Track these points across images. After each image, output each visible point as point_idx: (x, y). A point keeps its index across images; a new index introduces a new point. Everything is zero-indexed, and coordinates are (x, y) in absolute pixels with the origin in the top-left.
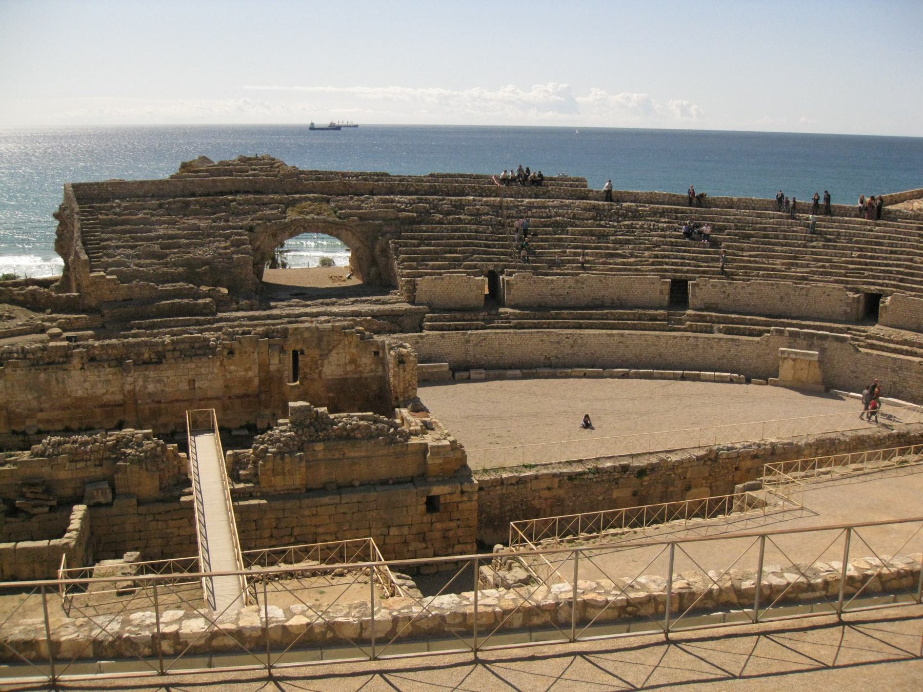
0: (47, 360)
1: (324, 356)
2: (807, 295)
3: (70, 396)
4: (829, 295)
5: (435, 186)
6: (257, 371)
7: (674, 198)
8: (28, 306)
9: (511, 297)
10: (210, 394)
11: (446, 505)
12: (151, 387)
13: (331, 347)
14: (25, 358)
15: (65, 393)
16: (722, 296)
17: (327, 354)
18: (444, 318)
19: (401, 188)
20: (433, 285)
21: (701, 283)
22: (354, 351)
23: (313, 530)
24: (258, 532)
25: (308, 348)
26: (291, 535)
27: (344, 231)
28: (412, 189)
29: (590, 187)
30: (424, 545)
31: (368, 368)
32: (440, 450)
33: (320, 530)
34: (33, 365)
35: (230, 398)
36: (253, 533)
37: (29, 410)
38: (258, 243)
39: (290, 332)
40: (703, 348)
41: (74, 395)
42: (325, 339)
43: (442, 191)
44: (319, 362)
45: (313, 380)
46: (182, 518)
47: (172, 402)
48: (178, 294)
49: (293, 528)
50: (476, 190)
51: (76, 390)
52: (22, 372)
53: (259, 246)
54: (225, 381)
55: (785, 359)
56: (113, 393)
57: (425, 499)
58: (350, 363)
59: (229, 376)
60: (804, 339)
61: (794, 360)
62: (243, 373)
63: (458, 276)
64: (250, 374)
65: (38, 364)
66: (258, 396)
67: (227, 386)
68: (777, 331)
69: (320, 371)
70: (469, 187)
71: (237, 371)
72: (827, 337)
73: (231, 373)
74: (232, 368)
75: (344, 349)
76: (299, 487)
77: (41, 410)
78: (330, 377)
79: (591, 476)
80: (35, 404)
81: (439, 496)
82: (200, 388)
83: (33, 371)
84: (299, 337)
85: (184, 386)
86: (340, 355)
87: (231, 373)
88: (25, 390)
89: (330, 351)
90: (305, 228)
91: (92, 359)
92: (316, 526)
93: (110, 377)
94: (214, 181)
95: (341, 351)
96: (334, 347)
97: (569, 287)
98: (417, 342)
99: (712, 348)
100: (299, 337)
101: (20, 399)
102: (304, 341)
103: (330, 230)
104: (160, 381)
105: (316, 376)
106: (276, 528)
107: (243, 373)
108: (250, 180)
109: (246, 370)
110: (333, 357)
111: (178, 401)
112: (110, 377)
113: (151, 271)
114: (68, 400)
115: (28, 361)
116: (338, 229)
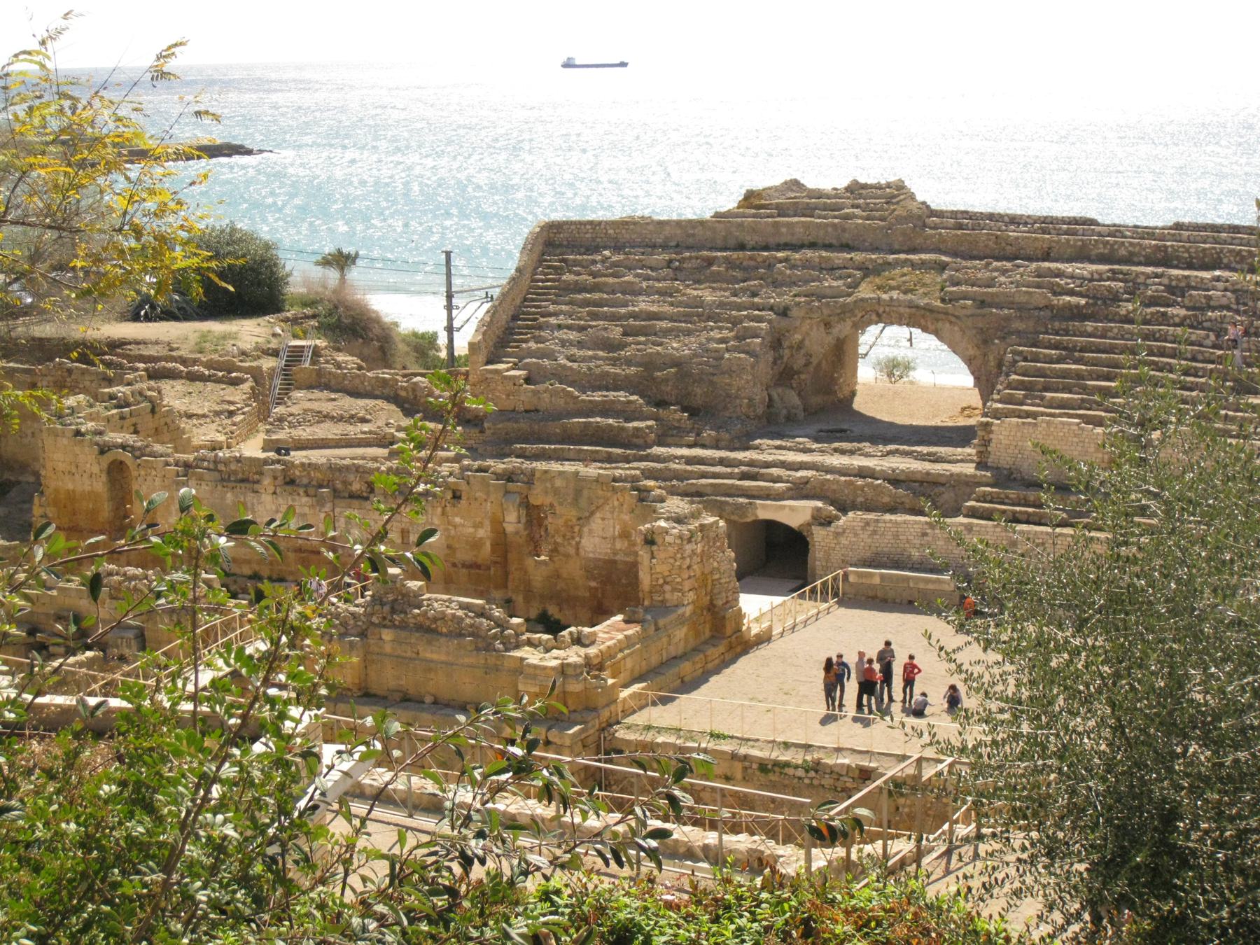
0: (240, 476)
1: (584, 519)
5: (1166, 247)
8: (406, 406)
13: (593, 507)
14: (216, 470)
17: (588, 518)
18: (1007, 497)
19: (1101, 250)
20: (1019, 434)
22: (626, 517)
25: (561, 504)
27: (948, 325)
28: (1123, 252)
32: (538, 672)
34: (223, 480)
38: (798, 337)
39: (537, 475)
42: (585, 493)
43: (1178, 258)
44: (576, 529)
45: (567, 556)
48: (605, 409)
53: (802, 342)
54: (448, 537)
62: (471, 530)
63: (1062, 423)
64: (481, 533)
65: (229, 480)
67: (449, 547)
69: (578, 543)
70: (1231, 251)
71: (463, 526)
73: (455, 527)
74: (458, 520)
75: (612, 513)
78: (591, 555)
79: (800, 773)
83: (219, 487)
89: (592, 513)
90: (878, 315)
91: (291, 482)
94: (776, 225)
95: (609, 515)
98: (924, 534)
100: (548, 485)
102: (556, 492)
103: (923, 323)
105: (572, 551)
107: (471, 530)
108: (834, 225)
110: (597, 523)
112: (306, 510)
113: (585, 369)
115: (216, 474)
116: (937, 320)
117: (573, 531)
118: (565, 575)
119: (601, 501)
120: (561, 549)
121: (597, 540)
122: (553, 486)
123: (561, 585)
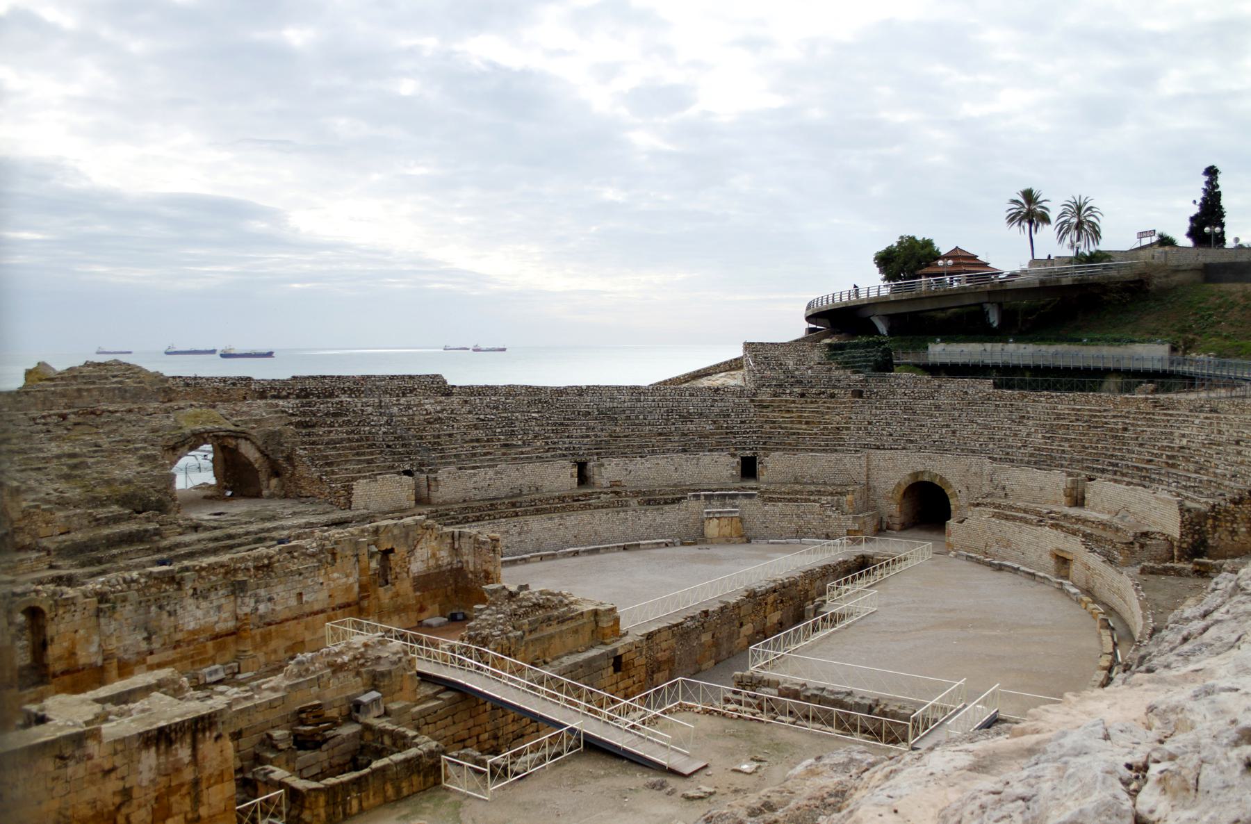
1: (411, 552)
2: (697, 464)
3: (182, 630)
4: (716, 462)
6: (357, 576)
7: (530, 390)
9: (439, 494)
10: (316, 607)
11: (627, 663)
12: (262, 608)
15: (176, 627)
16: (625, 473)
17: (413, 550)
21: (606, 463)
22: (434, 544)
25: (397, 546)
29: (450, 383)
31: (445, 561)
35: (333, 609)
37: (138, 653)
39: (382, 530)
40: (633, 520)
41: (186, 628)
42: (411, 533)
46: (446, 718)
47: (281, 622)
50: (345, 391)
51: (189, 622)
52: (131, 608)
54: (329, 590)
55: (711, 518)
56: (226, 620)
58: (431, 557)
59: (332, 586)
60: (718, 500)
61: (718, 518)
62: (345, 580)
66: (357, 603)
67: (330, 596)
68: (694, 496)
69: (408, 569)
72: (737, 495)
73: (334, 581)
74: (336, 575)
77: (151, 653)
80: (144, 646)
82: (307, 602)
84: (390, 534)
85: (293, 602)
87: (334, 581)
88: (135, 630)
89: (415, 546)
93: (223, 601)
97: (490, 479)
99: (639, 519)
100: (390, 534)
101: (127, 642)
102: (395, 538)
104: (270, 599)
109: (347, 576)
111: (287, 620)
114: (179, 636)
117: (406, 562)
118: (402, 594)
119: (420, 537)
120: (399, 576)
121: (419, 563)
122: (392, 535)
123: (400, 600)
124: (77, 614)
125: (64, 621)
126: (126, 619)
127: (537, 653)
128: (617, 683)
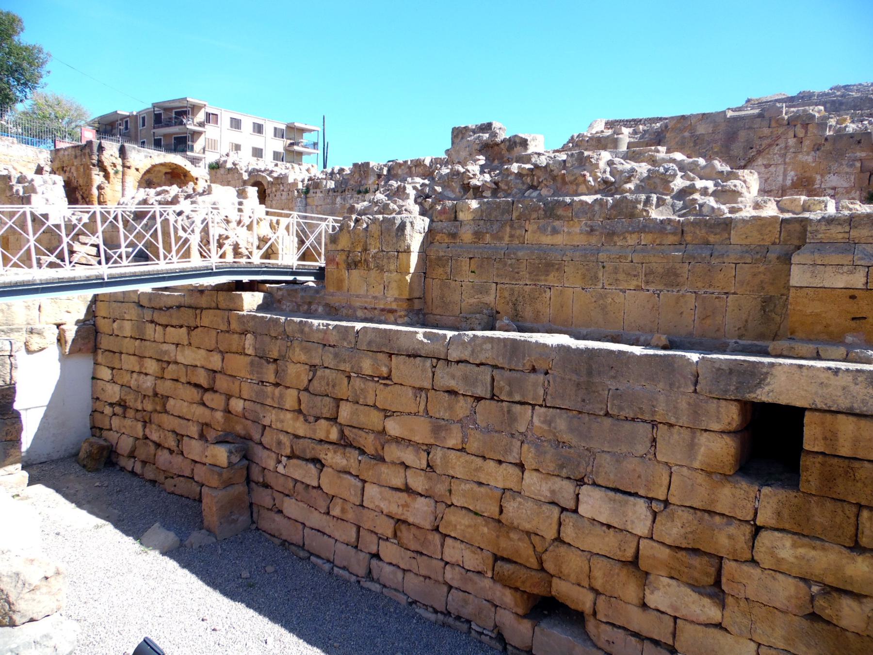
13: (753, 153)
23: (374, 419)
24: (277, 391)
26: (334, 419)
30: (713, 613)
33: (393, 427)
36: (270, 389)
42: (743, 135)
49: (338, 401)
52: (319, 195)
57: (731, 415)
75: (784, 156)
76: (394, 306)
81: (799, 412)
84: (687, 134)
86: (772, 169)
92: (387, 414)
95: (778, 159)
96: (759, 152)
100: (687, 134)
106: (306, 390)
119: (766, 142)
124: (284, 193)
125: (275, 198)
126: (317, 206)
127: (490, 299)
128: (757, 530)
